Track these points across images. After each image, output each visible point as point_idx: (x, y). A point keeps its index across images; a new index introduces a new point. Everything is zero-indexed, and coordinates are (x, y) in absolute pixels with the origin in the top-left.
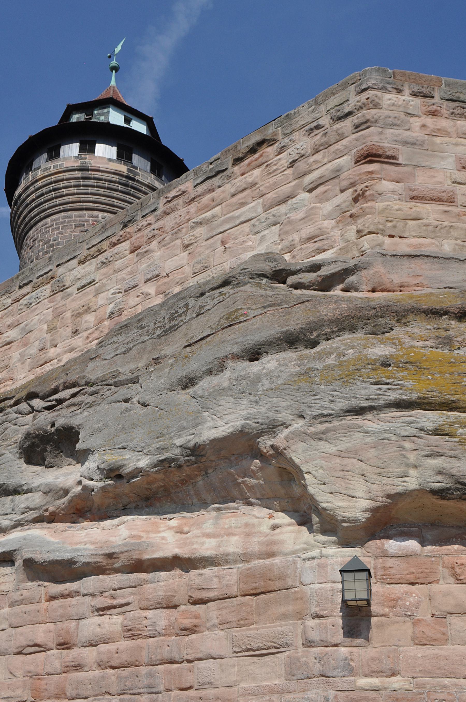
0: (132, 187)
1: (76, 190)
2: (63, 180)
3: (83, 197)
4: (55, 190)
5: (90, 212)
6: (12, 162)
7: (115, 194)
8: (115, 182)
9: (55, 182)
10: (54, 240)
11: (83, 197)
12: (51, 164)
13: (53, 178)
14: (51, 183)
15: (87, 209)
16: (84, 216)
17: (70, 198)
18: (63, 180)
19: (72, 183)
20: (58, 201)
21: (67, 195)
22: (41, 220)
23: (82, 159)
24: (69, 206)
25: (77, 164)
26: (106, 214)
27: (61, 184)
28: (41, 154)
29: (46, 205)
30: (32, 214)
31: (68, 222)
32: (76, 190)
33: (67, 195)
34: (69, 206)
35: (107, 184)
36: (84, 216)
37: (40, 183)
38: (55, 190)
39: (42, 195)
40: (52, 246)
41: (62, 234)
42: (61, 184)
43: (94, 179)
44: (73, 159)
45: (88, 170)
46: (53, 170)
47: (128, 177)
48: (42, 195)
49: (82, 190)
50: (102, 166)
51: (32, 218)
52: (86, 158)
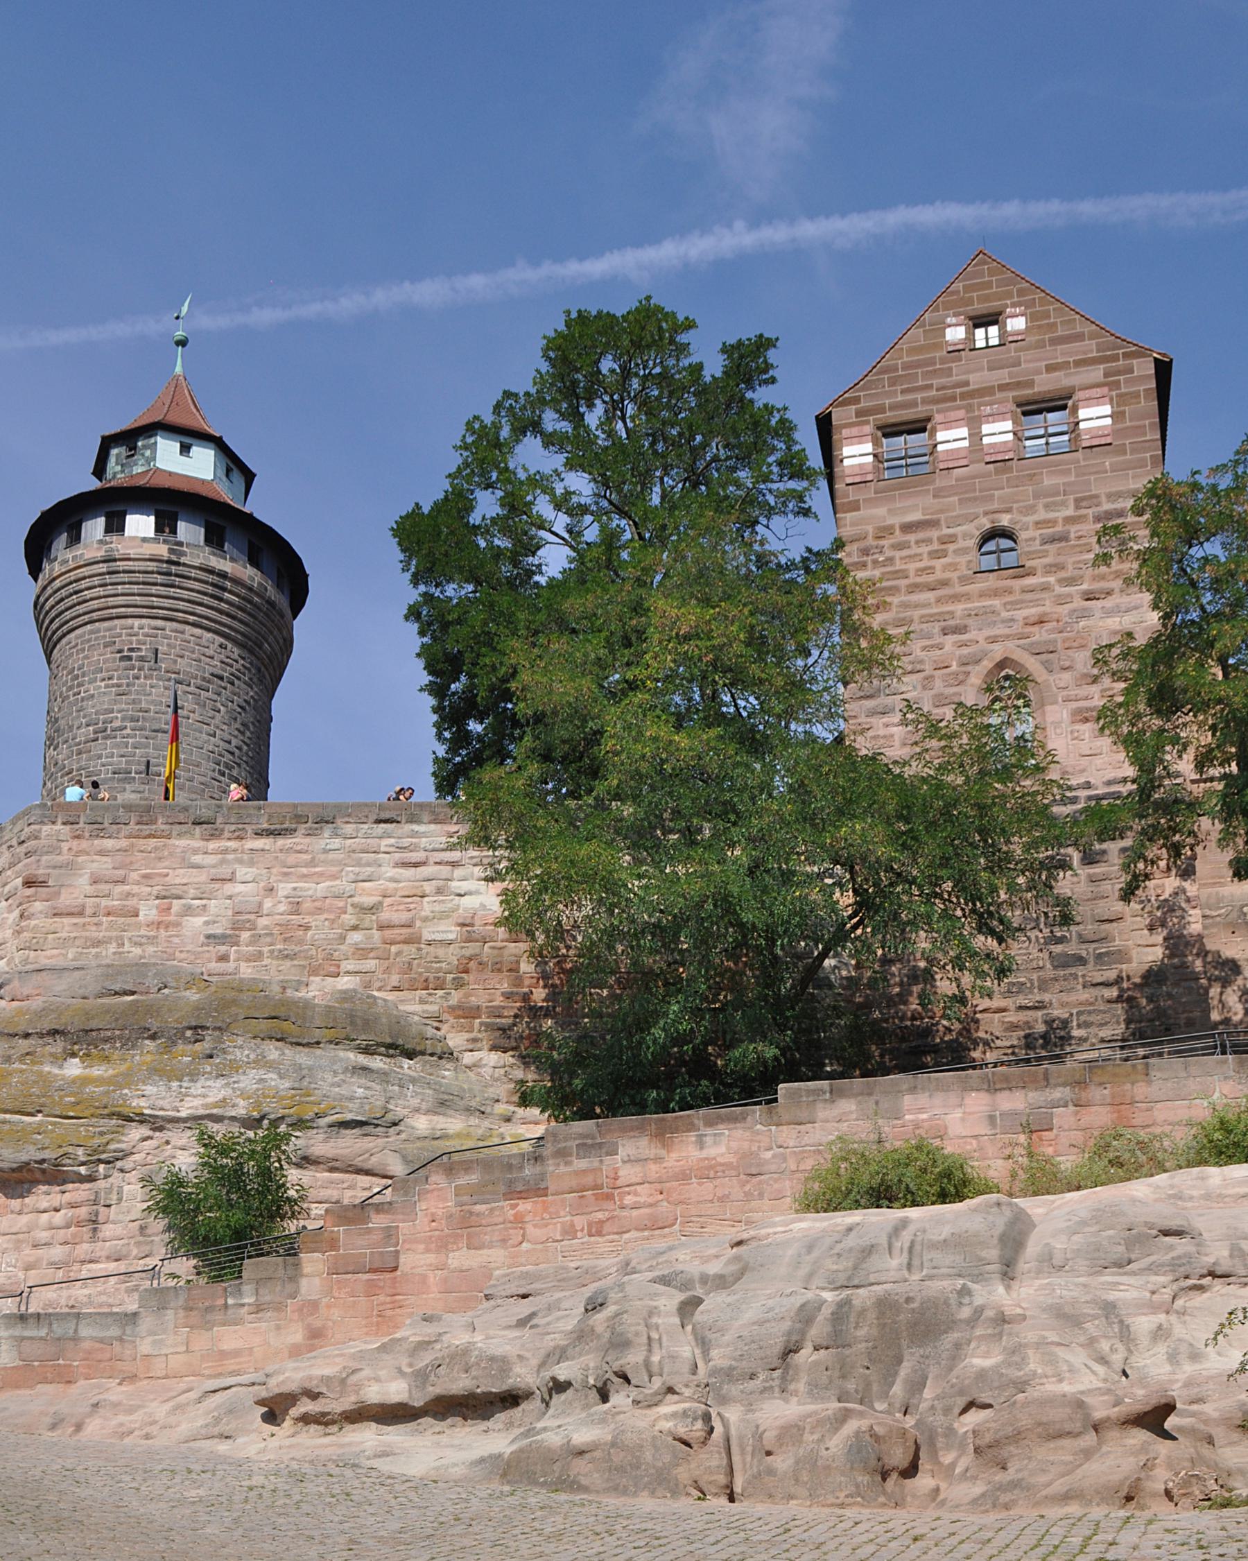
0: (177, 575)
3: (112, 601)
4: (76, 593)
5: (123, 621)
6: (45, 515)
7: (154, 590)
8: (152, 572)
9: (76, 581)
11: (112, 601)
12: (69, 555)
14: (71, 583)
15: (118, 617)
16: (115, 628)
17: (95, 604)
19: (96, 581)
20: (81, 609)
21: (92, 599)
22: (64, 635)
24: (95, 615)
25: (100, 554)
26: (144, 621)
27: (84, 584)
28: (61, 534)
29: (68, 615)
30: (54, 626)
33: (92, 599)
34: (95, 615)
35: (141, 578)
36: (115, 628)
37: (57, 584)
38: (76, 593)
39: (62, 600)
42: (84, 584)
43: (125, 572)
44: (95, 546)
45: (115, 560)
46: (72, 565)
48: (62, 600)
49: (110, 590)
50: (132, 553)
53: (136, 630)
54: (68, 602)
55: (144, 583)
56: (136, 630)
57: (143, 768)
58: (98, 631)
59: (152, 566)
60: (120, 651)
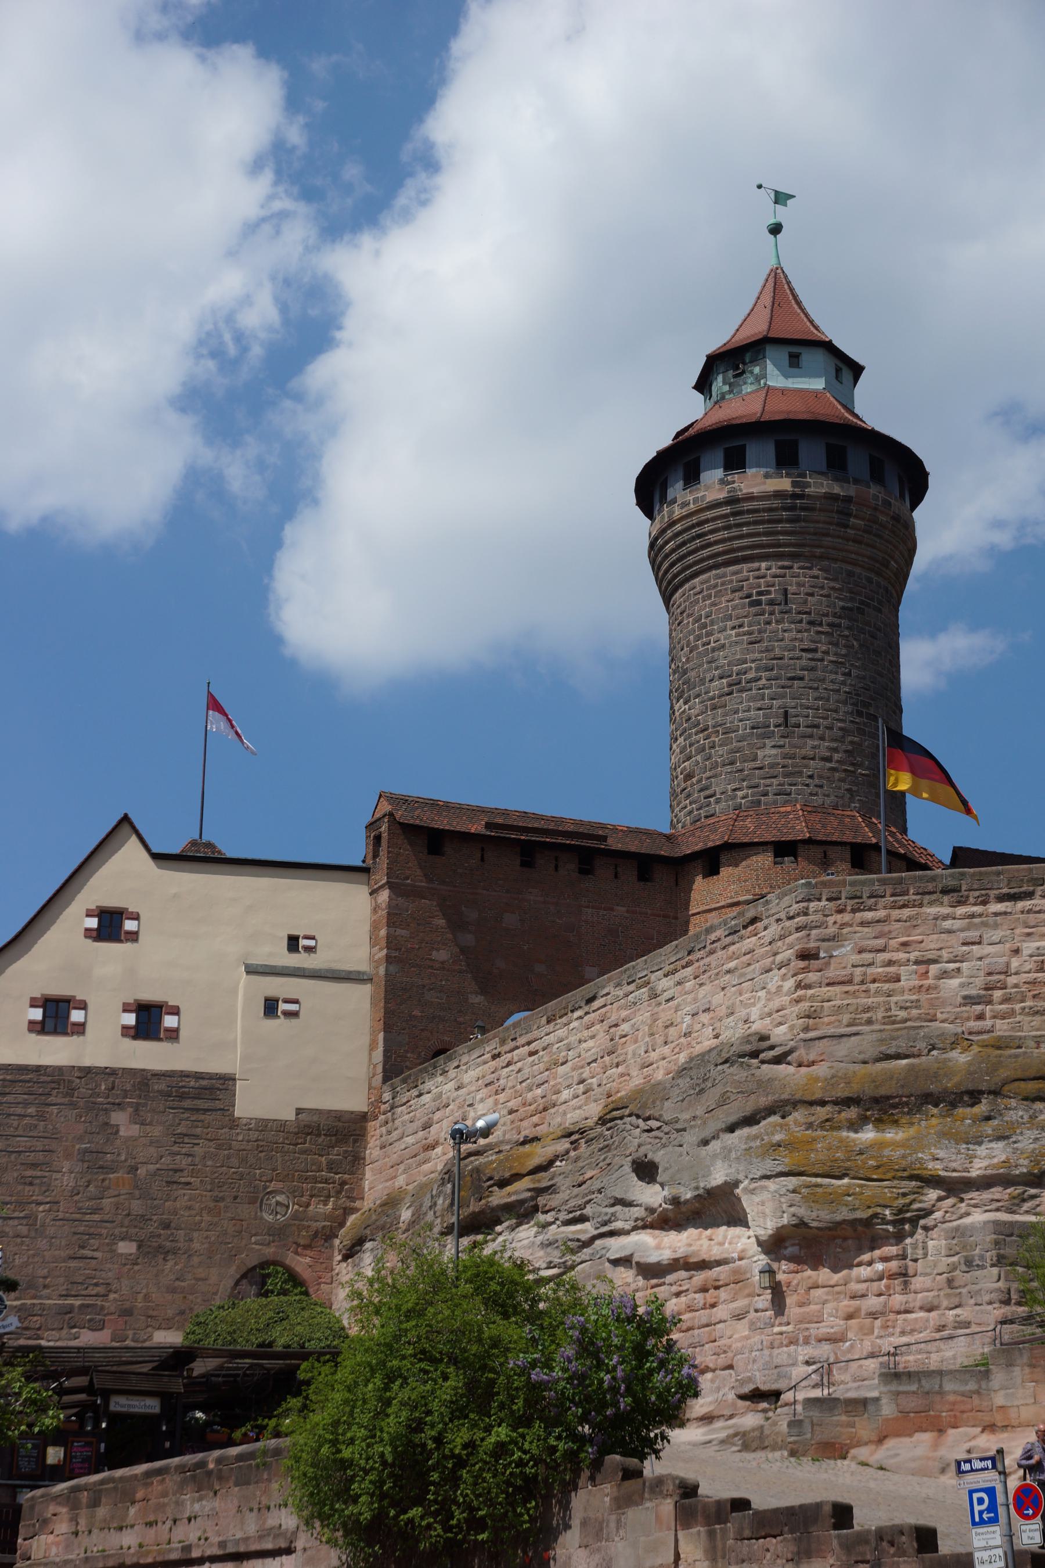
1: (725, 534)
2: (707, 521)
4: (699, 536)
9: (700, 524)
10: (707, 617)
13: (695, 520)
14: (693, 526)
17: (720, 548)
18: (707, 521)
19: (720, 524)
21: (716, 543)
23: (729, 483)
25: (722, 495)
27: (707, 527)
29: (691, 559)
30: (675, 569)
31: (723, 584)
32: (725, 534)
38: (699, 536)
39: (684, 544)
40: (705, 626)
41: (716, 605)
42: (707, 527)
43: (749, 512)
44: (717, 487)
46: (692, 507)
47: (794, 496)
49: (735, 532)
51: (675, 576)
52: (733, 482)
53: (763, 571)
54: (691, 546)
55: (769, 522)
56: (763, 571)
57: (792, 720)
58: (724, 575)
59: (776, 503)
60: (749, 596)
